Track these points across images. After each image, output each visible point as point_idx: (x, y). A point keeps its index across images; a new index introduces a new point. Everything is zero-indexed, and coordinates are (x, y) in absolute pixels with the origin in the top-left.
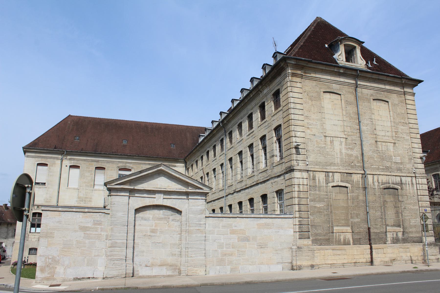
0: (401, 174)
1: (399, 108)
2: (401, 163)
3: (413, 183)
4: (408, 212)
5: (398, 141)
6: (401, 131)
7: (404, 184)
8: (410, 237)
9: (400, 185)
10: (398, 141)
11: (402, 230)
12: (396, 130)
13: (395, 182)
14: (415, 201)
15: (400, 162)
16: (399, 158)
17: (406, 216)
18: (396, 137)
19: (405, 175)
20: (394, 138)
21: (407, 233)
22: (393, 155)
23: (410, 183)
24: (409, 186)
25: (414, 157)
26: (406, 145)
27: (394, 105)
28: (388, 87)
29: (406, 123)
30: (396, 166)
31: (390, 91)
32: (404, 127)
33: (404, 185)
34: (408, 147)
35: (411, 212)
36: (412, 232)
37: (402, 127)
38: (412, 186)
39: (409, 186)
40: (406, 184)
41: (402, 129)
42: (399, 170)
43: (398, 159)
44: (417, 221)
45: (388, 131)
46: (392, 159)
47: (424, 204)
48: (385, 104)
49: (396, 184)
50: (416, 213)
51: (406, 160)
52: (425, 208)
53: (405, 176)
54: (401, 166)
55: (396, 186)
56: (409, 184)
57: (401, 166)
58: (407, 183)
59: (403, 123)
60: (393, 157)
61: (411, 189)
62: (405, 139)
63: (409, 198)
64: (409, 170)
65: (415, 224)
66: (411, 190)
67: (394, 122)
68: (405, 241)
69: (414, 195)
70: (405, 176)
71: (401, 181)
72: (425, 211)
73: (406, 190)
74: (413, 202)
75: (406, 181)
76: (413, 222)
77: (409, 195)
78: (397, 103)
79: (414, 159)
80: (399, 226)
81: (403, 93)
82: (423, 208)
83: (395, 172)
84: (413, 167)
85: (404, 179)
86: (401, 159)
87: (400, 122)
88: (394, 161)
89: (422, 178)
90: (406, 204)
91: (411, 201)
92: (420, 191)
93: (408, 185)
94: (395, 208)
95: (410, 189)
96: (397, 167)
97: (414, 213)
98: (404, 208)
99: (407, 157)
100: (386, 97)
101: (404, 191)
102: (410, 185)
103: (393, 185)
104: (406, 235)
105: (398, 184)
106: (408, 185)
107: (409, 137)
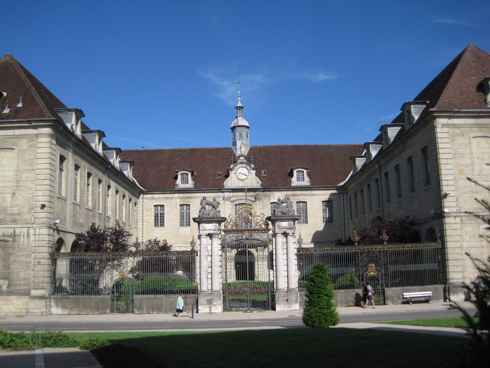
0: (14, 226)
1: (28, 154)
2: (19, 214)
3: (30, 234)
4: (18, 264)
5: (20, 190)
6: (25, 180)
7: (18, 236)
8: (16, 290)
9: (13, 237)
10: (20, 190)
11: (7, 282)
12: (18, 179)
13: (6, 234)
14: (28, 253)
15: (17, 212)
16: (17, 208)
17: (15, 268)
18: (17, 186)
19: (20, 226)
20: (15, 188)
21: (14, 285)
22: (8, 205)
23: (26, 234)
24: (24, 238)
25: (35, 206)
26: (28, 194)
27: (22, 151)
28: (18, 132)
29: (34, 170)
30: (11, 218)
31: (19, 136)
32: (29, 175)
33: (17, 237)
34: (31, 196)
35: (21, 264)
36: (19, 285)
37: (28, 175)
38: (27, 237)
39: (24, 238)
40: (20, 235)
41: (26, 177)
42: (15, 221)
43: (15, 210)
44: (27, 273)
45: (9, 182)
46: (7, 211)
47: (38, 256)
48: (11, 152)
49: (8, 236)
50: (28, 265)
51: (26, 210)
52: (39, 260)
53: (20, 228)
54: (17, 217)
55: (7, 238)
56: (24, 235)
57: (17, 217)
58: (22, 234)
59: (30, 170)
60: (10, 209)
61: (26, 240)
62: (29, 187)
63: (22, 250)
64: (27, 220)
65: (25, 276)
66: (25, 242)
67: (17, 170)
68: (9, 293)
69: (29, 247)
70: (20, 228)
71: (14, 232)
72: (38, 263)
73: (20, 242)
74: (26, 254)
75: (21, 232)
76: (23, 274)
77: (21, 247)
78: (25, 148)
79: (35, 208)
80: (5, 278)
81: (35, 136)
82: (36, 260)
83: (9, 223)
84: (33, 218)
85: (18, 231)
86: (19, 210)
87: (26, 170)
88: (9, 212)
89: (41, 228)
90: (17, 256)
91: (24, 253)
92: (35, 243)
93: (22, 237)
94: (4, 261)
95: (24, 241)
96: (13, 218)
97: (26, 265)
98: (13, 261)
99: (27, 206)
100: (13, 144)
101: (16, 244)
102: (26, 237)
103: (3, 238)
104: (11, 288)
105: (11, 236)
106: (22, 237)
107: (34, 185)
